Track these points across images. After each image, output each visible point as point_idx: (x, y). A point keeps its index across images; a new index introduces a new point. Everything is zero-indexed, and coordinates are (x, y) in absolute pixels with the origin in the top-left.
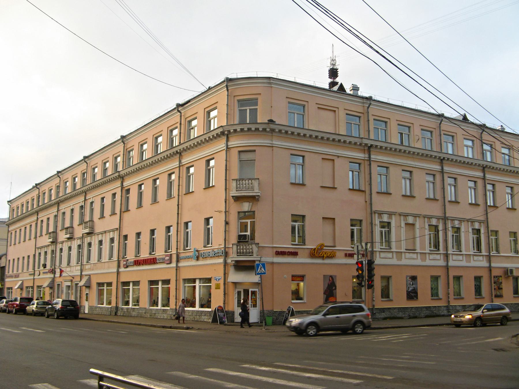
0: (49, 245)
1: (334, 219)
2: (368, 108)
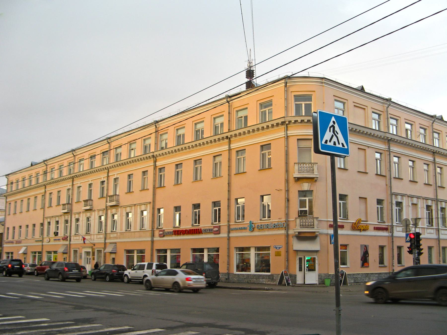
0: (61, 215)
1: (366, 198)
2: (388, 107)
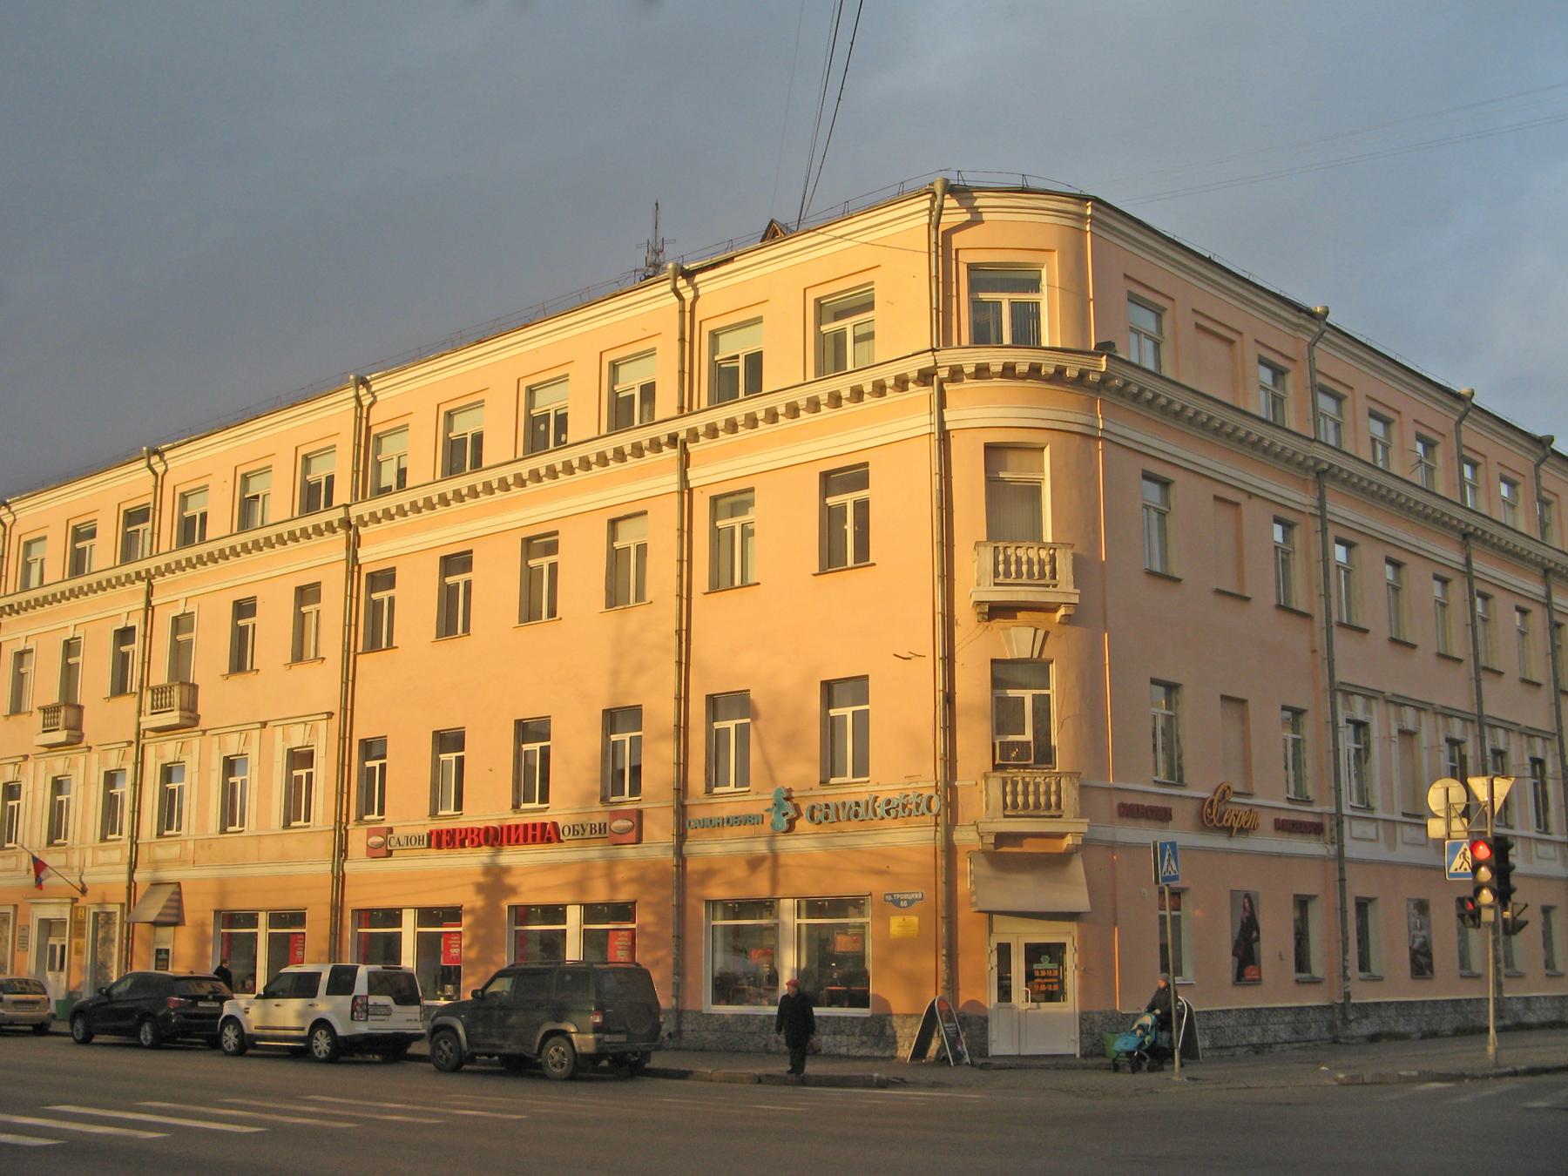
1: (1242, 702)
